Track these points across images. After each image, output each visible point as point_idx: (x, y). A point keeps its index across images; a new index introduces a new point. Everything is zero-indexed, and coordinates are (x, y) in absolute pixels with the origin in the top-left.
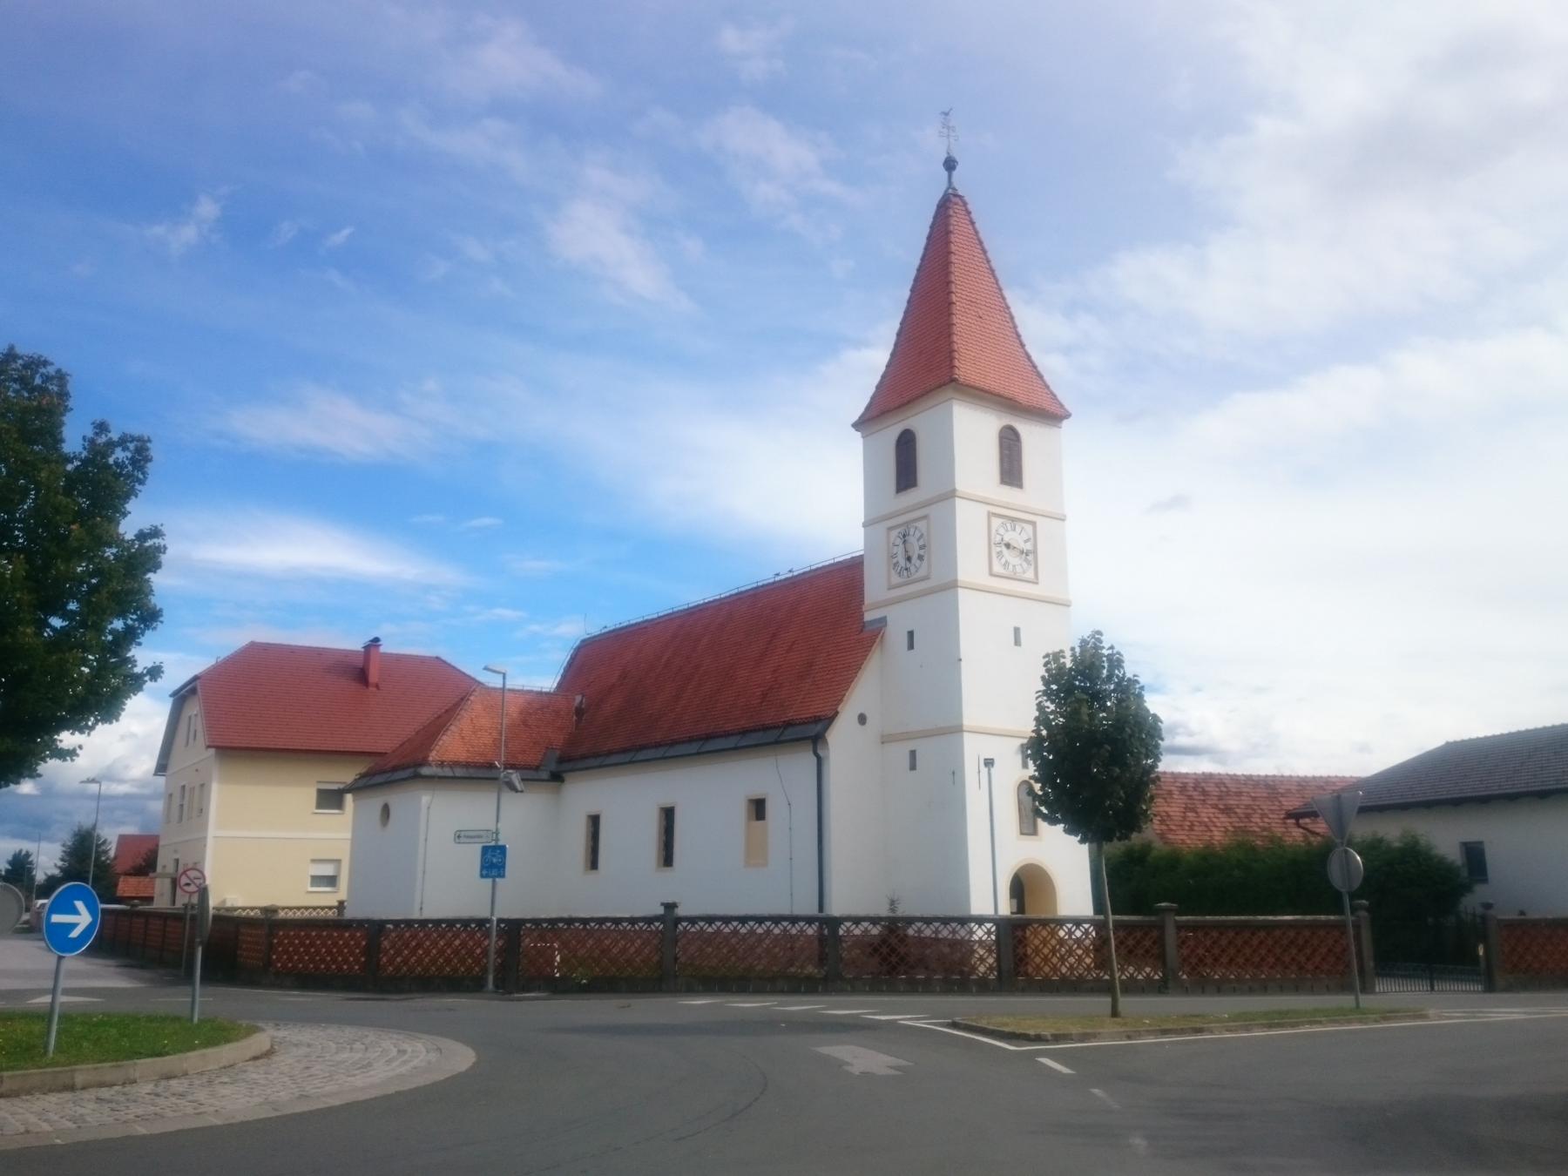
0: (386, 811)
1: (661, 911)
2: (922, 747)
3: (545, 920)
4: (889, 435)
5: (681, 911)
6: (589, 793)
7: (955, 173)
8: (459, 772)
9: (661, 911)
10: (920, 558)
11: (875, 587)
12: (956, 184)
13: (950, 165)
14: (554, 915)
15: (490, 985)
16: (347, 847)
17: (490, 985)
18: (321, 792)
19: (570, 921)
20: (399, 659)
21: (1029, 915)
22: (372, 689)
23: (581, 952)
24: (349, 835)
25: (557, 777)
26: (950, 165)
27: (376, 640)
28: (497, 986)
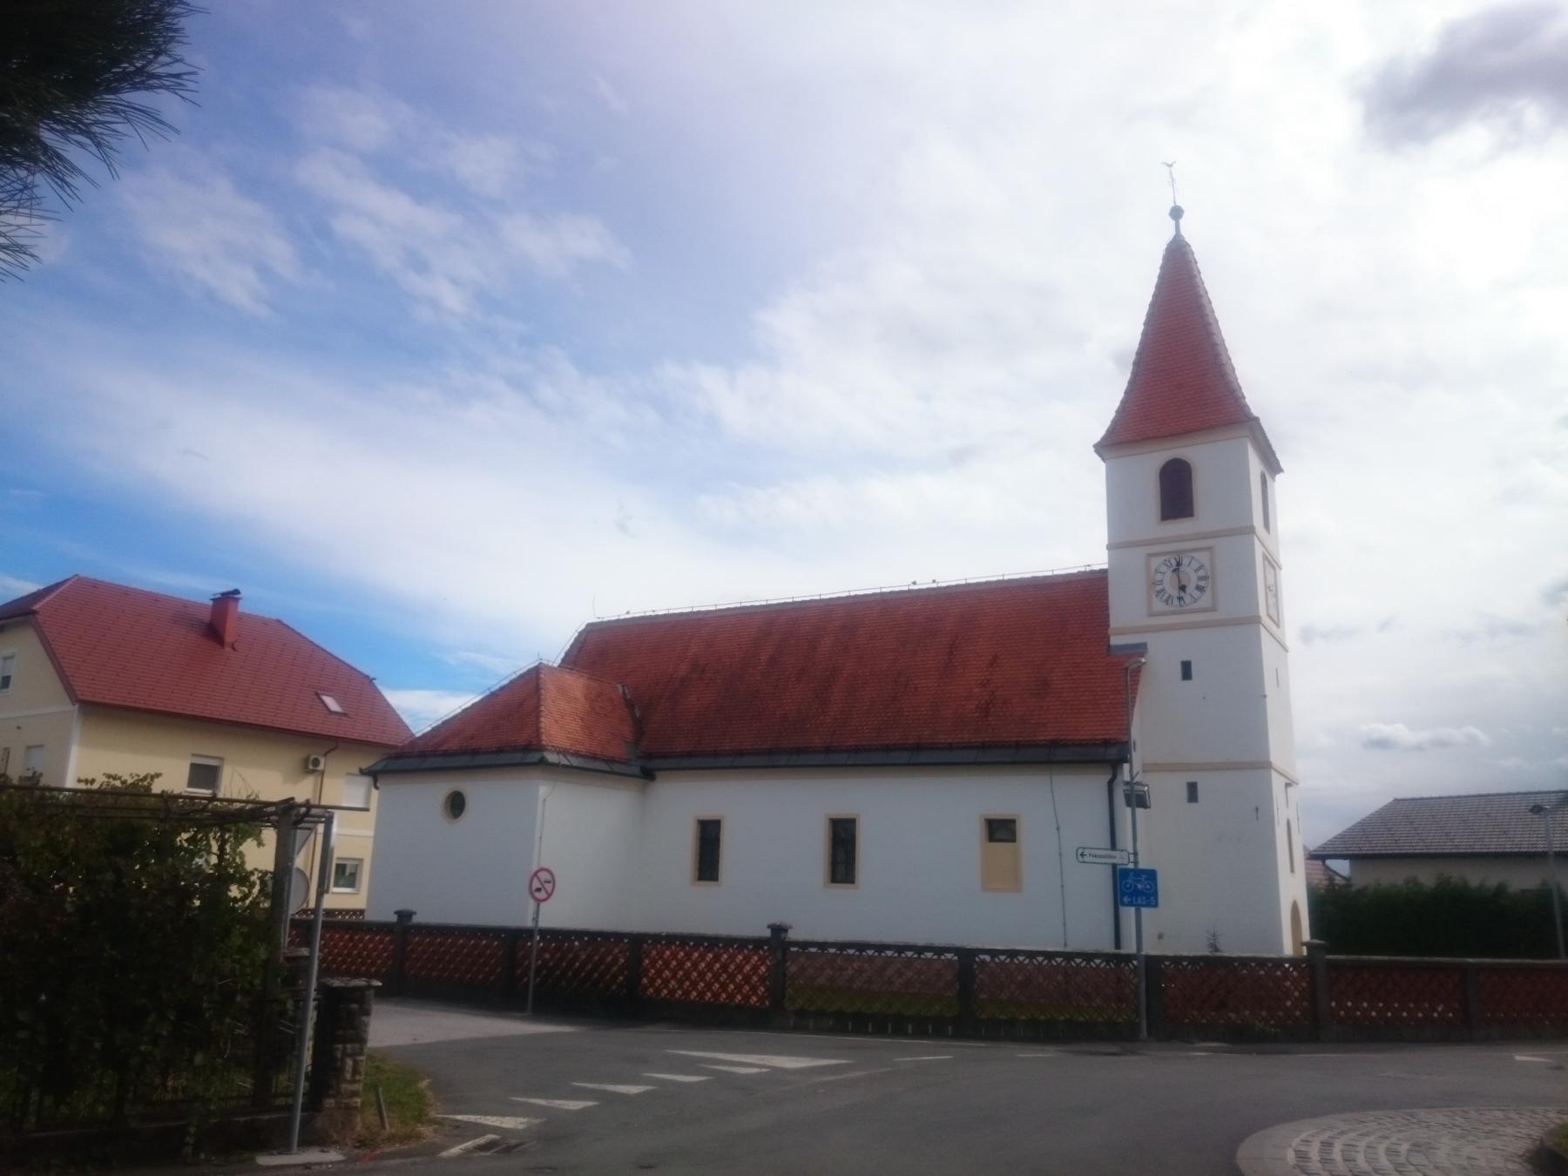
0: (456, 805)
1: (768, 933)
2: (1204, 782)
3: (833, 945)
4: (1150, 462)
5: (792, 935)
6: (686, 800)
7: (1182, 221)
8: (575, 762)
9: (768, 933)
10: (1200, 589)
11: (1127, 615)
12: (1183, 232)
13: (1176, 213)
14: (921, 941)
15: (1144, 1034)
16: (370, 845)
17: (1144, 1034)
18: (194, 767)
19: (861, 947)
20: (249, 616)
21: (1123, 951)
22: (228, 649)
23: (821, 980)
24: (371, 833)
25: (648, 775)
26: (1176, 213)
27: (237, 592)
28: (1149, 1033)
